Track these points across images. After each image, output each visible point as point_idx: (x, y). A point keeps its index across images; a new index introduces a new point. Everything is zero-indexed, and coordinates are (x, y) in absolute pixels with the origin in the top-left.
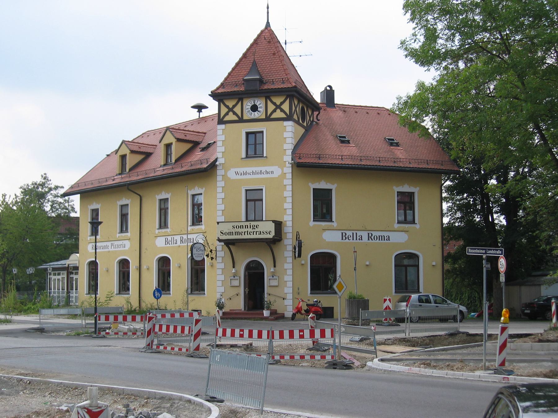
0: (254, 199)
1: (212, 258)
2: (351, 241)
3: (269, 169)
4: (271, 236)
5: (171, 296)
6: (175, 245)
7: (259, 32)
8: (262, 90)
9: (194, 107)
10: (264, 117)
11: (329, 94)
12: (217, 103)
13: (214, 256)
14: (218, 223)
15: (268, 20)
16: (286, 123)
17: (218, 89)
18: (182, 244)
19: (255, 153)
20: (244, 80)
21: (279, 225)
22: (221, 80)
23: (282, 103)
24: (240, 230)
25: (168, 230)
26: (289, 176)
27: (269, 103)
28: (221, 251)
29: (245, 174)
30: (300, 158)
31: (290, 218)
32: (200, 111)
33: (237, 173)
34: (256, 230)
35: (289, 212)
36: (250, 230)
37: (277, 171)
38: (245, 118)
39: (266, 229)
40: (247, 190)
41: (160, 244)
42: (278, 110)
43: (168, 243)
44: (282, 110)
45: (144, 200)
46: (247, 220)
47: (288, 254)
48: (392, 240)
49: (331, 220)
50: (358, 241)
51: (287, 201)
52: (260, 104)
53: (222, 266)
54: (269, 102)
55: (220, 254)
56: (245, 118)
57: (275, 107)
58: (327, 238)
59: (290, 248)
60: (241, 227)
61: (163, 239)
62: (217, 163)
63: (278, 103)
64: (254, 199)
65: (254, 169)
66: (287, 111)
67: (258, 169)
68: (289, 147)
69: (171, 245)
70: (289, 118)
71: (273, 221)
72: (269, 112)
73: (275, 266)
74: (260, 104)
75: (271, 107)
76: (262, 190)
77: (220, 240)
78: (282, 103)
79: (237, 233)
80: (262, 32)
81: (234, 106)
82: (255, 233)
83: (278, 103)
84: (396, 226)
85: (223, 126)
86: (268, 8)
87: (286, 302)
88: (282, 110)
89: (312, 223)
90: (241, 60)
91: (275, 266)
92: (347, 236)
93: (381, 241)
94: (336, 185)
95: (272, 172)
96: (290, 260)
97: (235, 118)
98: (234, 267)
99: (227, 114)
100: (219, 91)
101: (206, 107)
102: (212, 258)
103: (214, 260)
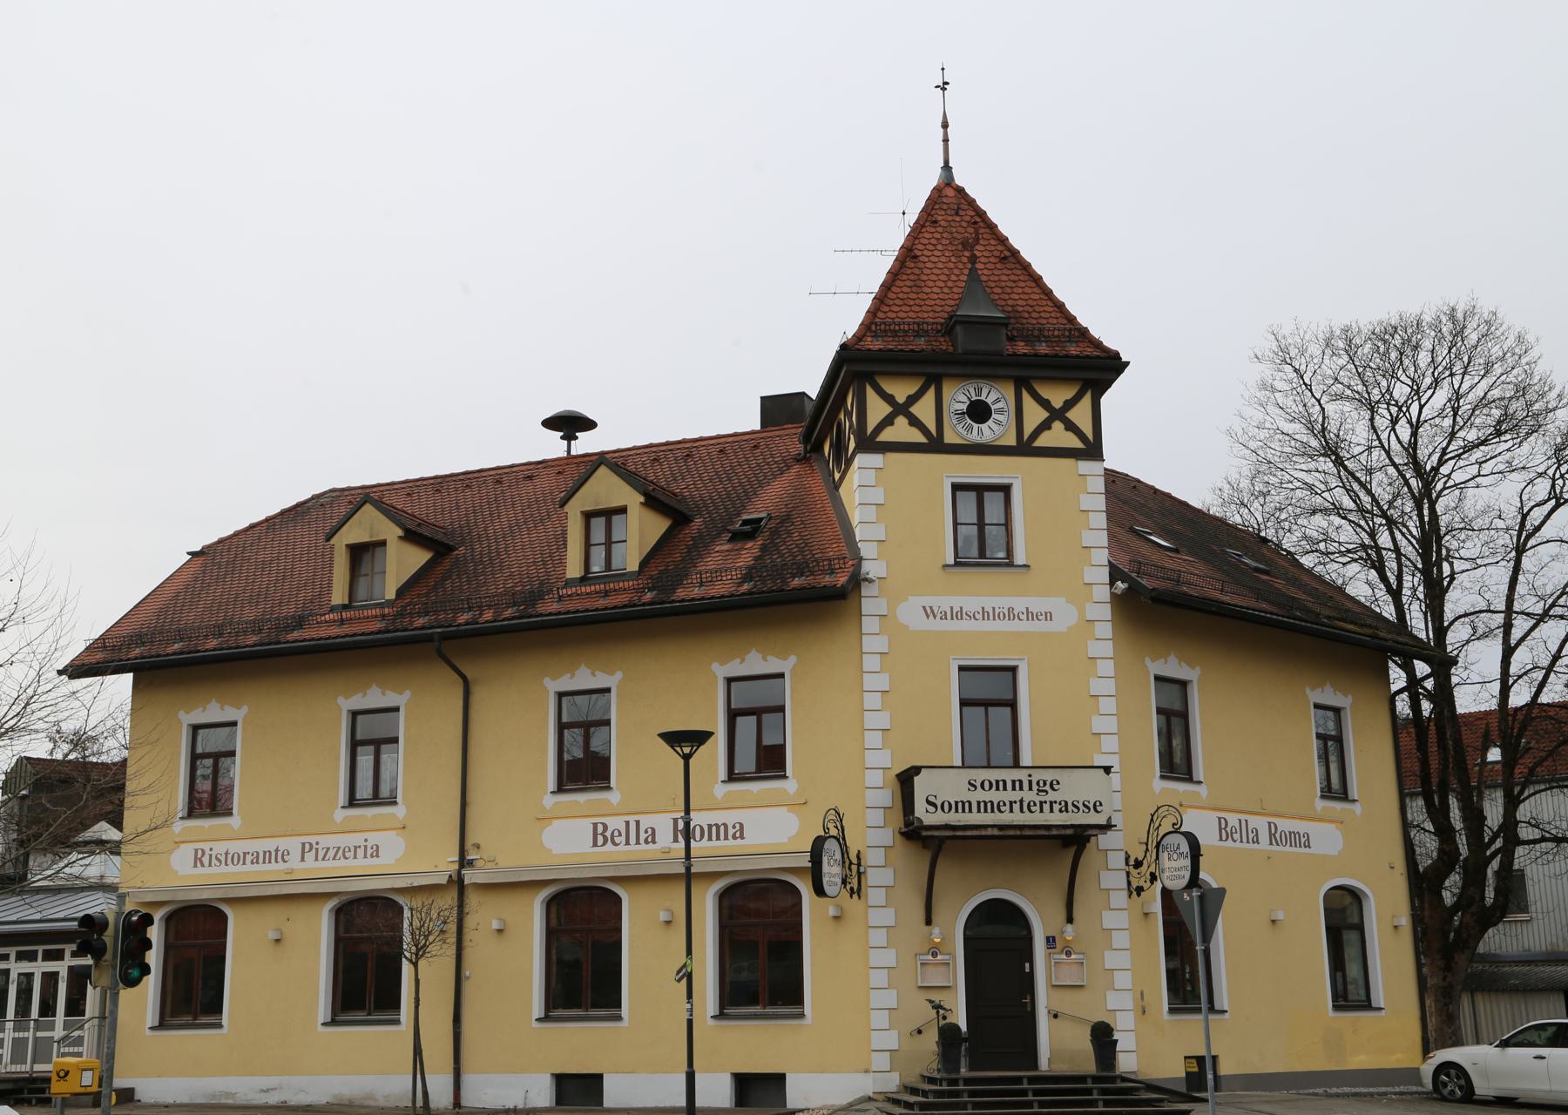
0: (990, 695)
3: (1036, 604)
5: (625, 1023)
10: (1011, 441)
15: (946, 162)
24: (994, 796)
25: (613, 797)
27: (1027, 399)
29: (959, 615)
32: (569, 437)
33: (929, 612)
34: (1052, 796)
36: (1029, 796)
38: (950, 438)
40: (961, 669)
41: (569, 839)
42: (1058, 426)
45: (478, 695)
47: (1114, 879)
48: (1316, 848)
52: (998, 401)
53: (887, 917)
54: (1026, 397)
55: (878, 877)
56: (950, 438)
57: (1045, 414)
63: (1057, 403)
64: (990, 695)
65: (989, 603)
67: (1002, 603)
72: (1028, 429)
74: (998, 401)
75: (1034, 415)
76: (1013, 670)
79: (984, 806)
82: (1046, 807)
83: (1057, 403)
84: (1320, 804)
85: (875, 459)
86: (945, 125)
88: (1071, 427)
91: (1070, 920)
93: (1293, 849)
95: (1049, 616)
96: (1119, 899)
101: (588, 424)
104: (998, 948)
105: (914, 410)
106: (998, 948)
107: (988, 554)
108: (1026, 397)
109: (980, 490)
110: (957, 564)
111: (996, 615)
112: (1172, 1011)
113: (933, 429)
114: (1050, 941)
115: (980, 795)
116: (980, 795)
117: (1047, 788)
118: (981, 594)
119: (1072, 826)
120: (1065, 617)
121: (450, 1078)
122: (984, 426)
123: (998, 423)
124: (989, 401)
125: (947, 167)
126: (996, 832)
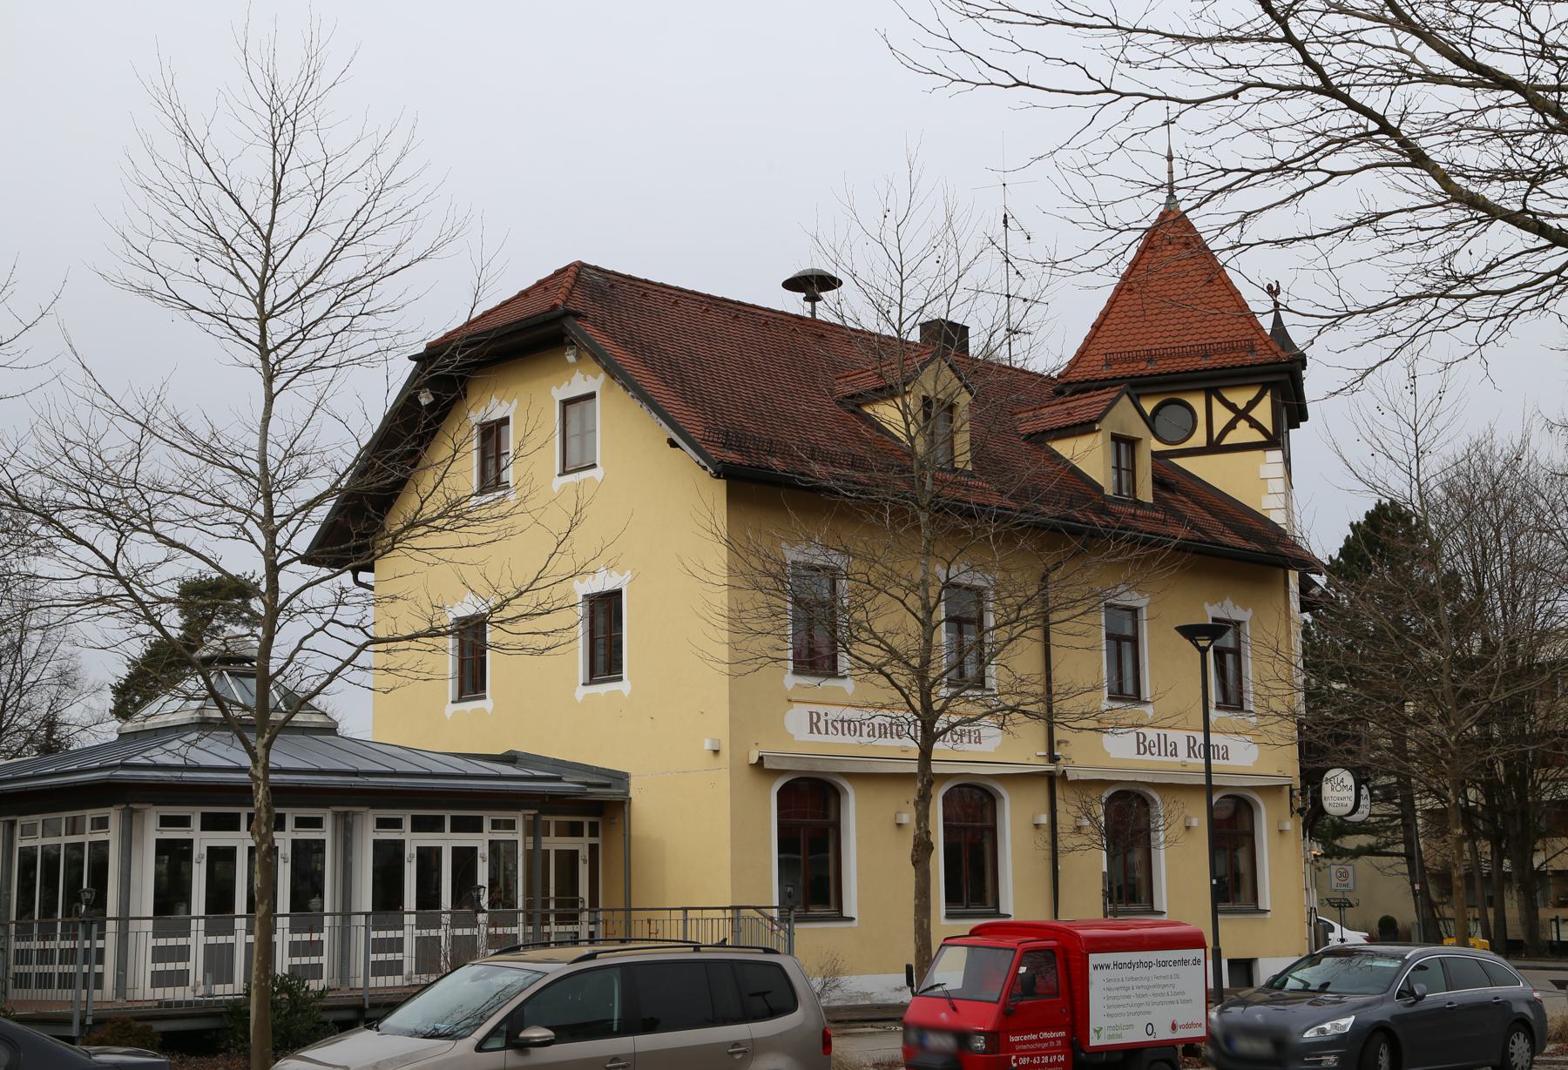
6: (1169, 758)
23: (1252, 404)
27: (1216, 403)
44: (1254, 424)
54: (1215, 402)
63: (1241, 405)
69: (1156, 758)
72: (1216, 435)
75: (1222, 416)
78: (1252, 404)
83: (1241, 405)
88: (1254, 424)
108: (1215, 402)
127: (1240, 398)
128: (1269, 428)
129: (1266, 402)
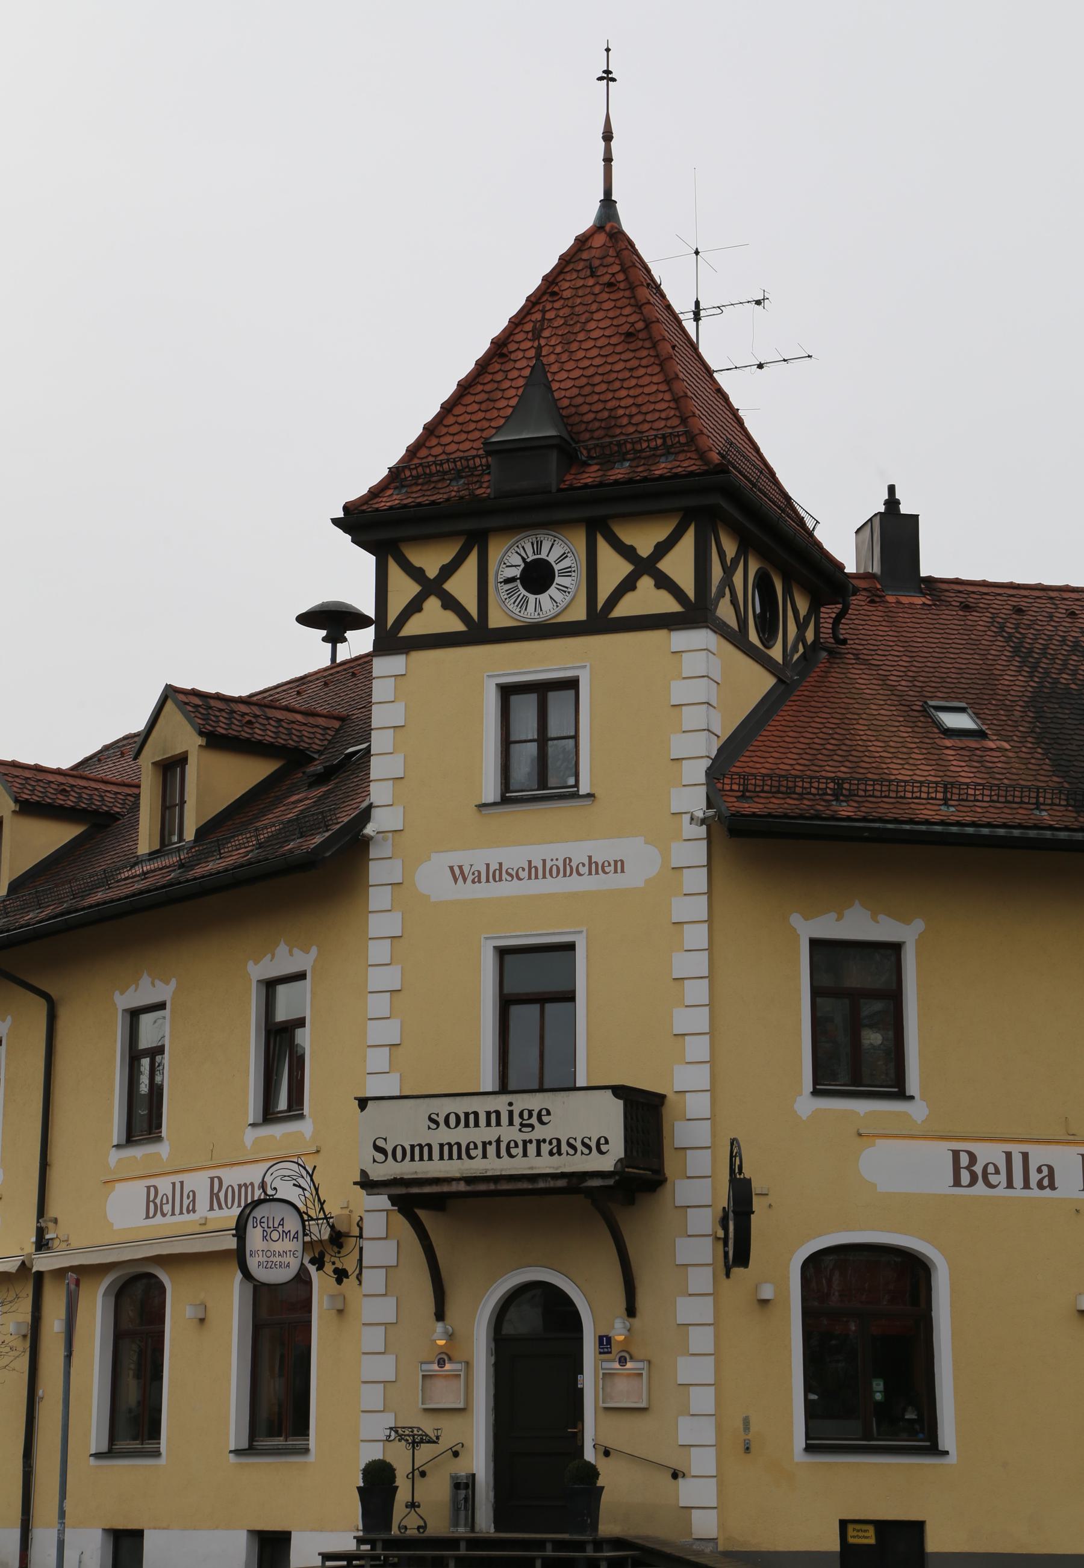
0: (535, 986)
1: (341, 1275)
2: (1001, 1191)
3: (603, 850)
4: (606, 1163)
7: (566, 244)
8: (572, 488)
9: (308, 619)
10: (579, 613)
11: (895, 530)
12: (372, 559)
13: (349, 1264)
14: (363, 1103)
15: (608, 192)
16: (681, 639)
17: (375, 493)
18: (217, 1213)
19: (543, 783)
20: (493, 450)
21: (645, 1111)
22: (395, 455)
24: (462, 1135)
25: (163, 1150)
26: (698, 880)
27: (604, 548)
28: (383, 1241)
29: (496, 874)
30: (743, 797)
31: (700, 1078)
32: (335, 638)
33: (458, 874)
35: (698, 1048)
36: (509, 1133)
37: (641, 861)
38: (497, 620)
39: (587, 1129)
40: (503, 953)
41: (120, 1210)
42: (646, 583)
43: (159, 1210)
44: (664, 582)
46: (504, 1088)
49: (901, 1094)
50: (1035, 1192)
51: (692, 999)
52: (563, 557)
56: (497, 620)
58: (881, 1175)
59: (704, 1221)
60: (469, 1119)
61: (139, 1188)
62: (369, 830)
63: (645, 550)
64: (535, 986)
65: (537, 853)
66: (687, 583)
67: (556, 852)
68: (695, 748)
69: (169, 1219)
70: (695, 613)
71: (618, 1091)
72: (603, 595)
73: (631, 1311)
74: (563, 557)
75: (613, 569)
76: (571, 947)
77: (367, 1184)
78: (663, 549)
79: (450, 1150)
80: (582, 242)
81: (448, 571)
82: (532, 1149)
83: (645, 550)
86: (608, 136)
87: (688, 1492)
88: (664, 582)
89: (807, 1105)
90: (483, 366)
91: (631, 1311)
92: (978, 1169)
94: (918, 925)
95: (619, 866)
96: (702, 1279)
97: (453, 624)
98: (440, 1316)
99: (415, 607)
100: (384, 503)
102: (341, 1275)
103: (350, 1282)
104: (538, 1358)
105: (450, 586)
106: (538, 1358)
107: (552, 781)
109: (542, 689)
110: (506, 800)
111: (546, 871)
112: (809, 1449)
113: (473, 609)
114: (605, 1343)
115: (444, 1135)
116: (444, 1135)
117: (534, 1121)
118: (537, 839)
119: (563, 1175)
120: (641, 861)
121: (16, 1534)
122: (544, 598)
123: (563, 590)
124: (551, 559)
125: (608, 203)
126: (462, 1187)
127: (644, 539)
128: (691, 593)
129: (687, 544)
